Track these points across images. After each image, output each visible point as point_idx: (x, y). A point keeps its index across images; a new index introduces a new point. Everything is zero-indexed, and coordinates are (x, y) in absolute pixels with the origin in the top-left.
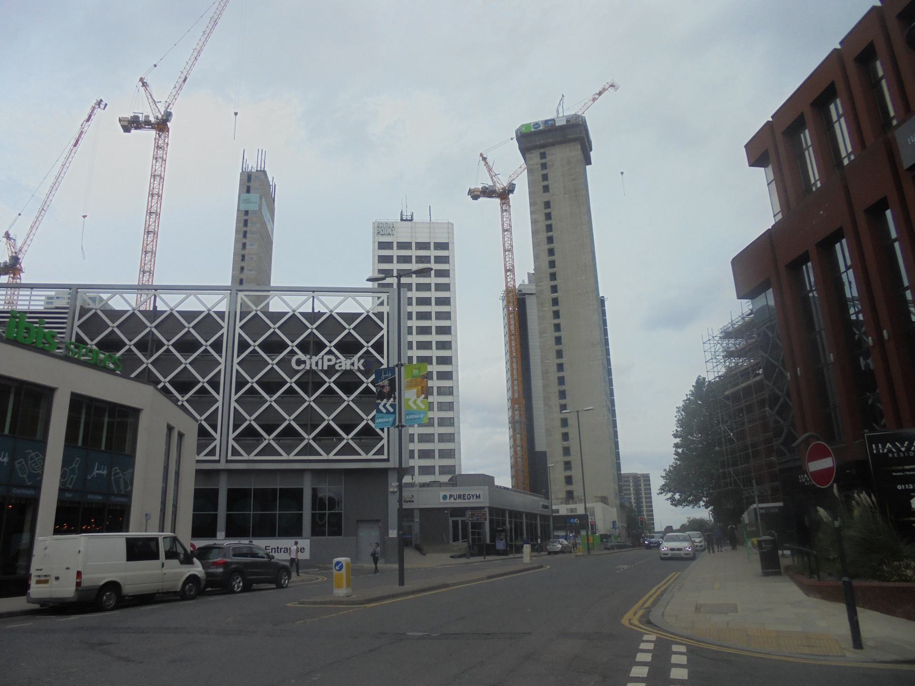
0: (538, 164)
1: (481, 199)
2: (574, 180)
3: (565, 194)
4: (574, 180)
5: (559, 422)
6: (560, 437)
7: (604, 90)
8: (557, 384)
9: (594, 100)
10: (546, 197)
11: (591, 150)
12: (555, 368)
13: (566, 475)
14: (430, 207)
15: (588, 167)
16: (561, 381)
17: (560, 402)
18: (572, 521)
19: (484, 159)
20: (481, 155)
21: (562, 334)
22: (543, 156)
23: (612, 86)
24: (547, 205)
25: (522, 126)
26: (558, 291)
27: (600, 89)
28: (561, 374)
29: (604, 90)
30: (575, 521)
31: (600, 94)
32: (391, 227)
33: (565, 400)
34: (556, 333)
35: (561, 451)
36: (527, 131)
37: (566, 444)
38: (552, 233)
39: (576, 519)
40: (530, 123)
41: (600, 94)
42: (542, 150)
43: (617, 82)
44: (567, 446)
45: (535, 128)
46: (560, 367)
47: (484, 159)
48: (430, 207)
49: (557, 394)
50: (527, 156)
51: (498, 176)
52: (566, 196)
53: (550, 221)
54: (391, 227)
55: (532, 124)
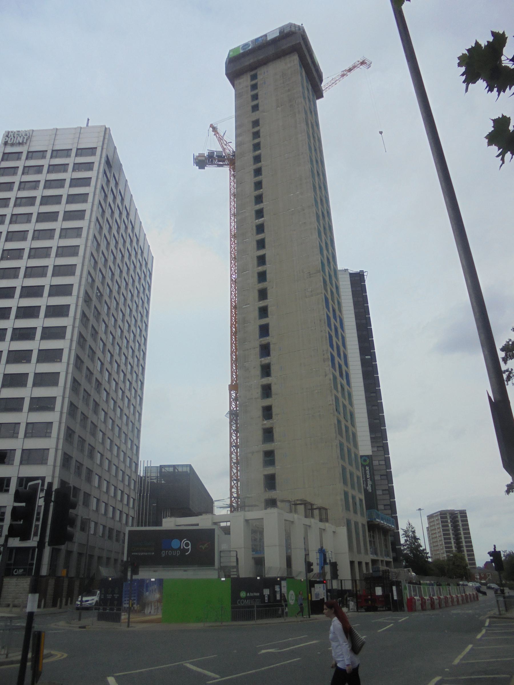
0: (247, 87)
1: (210, 169)
2: (289, 90)
3: (278, 107)
4: (289, 90)
5: (259, 390)
6: (259, 413)
7: (354, 67)
8: (258, 335)
9: (343, 75)
10: (255, 116)
11: (321, 81)
12: (256, 313)
13: (266, 473)
14: (88, 120)
15: (319, 102)
16: (264, 330)
17: (261, 361)
18: (175, 543)
19: (214, 129)
20: (211, 126)
21: (268, 267)
22: (254, 77)
23: (363, 63)
24: (256, 123)
25: (230, 51)
26: (265, 216)
27: (350, 66)
28: (264, 321)
29: (354, 67)
30: (183, 545)
31: (350, 70)
32: (23, 135)
33: (269, 358)
34: (260, 268)
35: (259, 435)
36: (236, 54)
37: (267, 423)
38: (260, 151)
39: (185, 541)
40: (239, 46)
41: (350, 70)
42: (253, 73)
43: (369, 58)
44: (268, 426)
45: (244, 49)
46: (263, 312)
47: (214, 129)
48: (88, 120)
49: (258, 350)
50: (236, 82)
51: (229, 144)
52: (279, 108)
53: (259, 139)
54: (23, 135)
55: (241, 47)
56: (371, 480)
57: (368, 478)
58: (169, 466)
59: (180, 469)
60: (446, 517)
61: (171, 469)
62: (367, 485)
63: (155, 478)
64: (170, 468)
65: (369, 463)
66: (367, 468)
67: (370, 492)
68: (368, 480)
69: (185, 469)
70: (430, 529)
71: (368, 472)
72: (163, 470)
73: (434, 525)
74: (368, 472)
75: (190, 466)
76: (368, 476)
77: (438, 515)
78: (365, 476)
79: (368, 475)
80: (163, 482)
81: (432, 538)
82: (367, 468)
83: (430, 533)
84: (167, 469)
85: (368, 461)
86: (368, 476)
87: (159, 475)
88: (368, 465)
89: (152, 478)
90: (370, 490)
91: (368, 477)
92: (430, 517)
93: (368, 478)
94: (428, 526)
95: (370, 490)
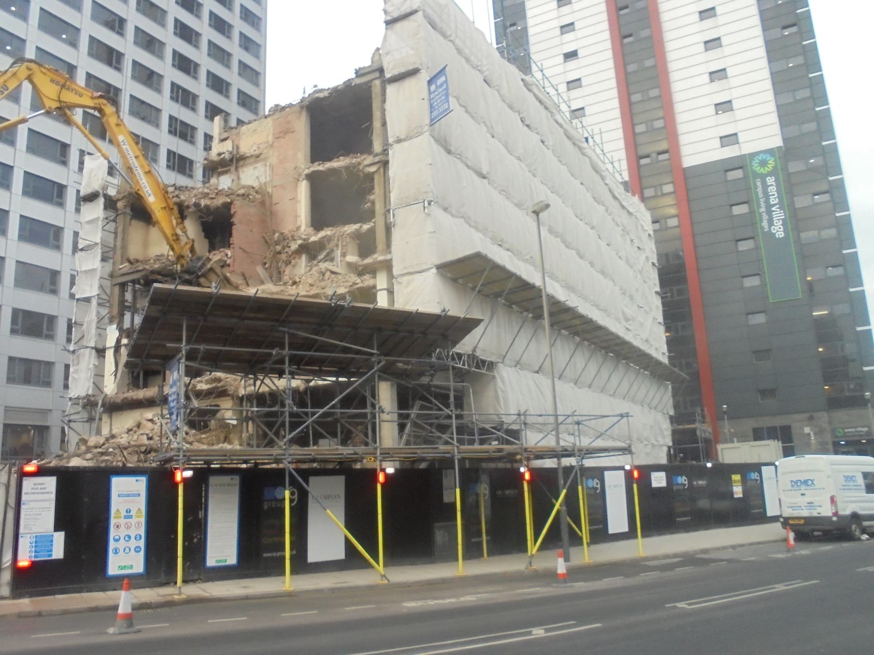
57: (775, 205)
62: (771, 223)
65: (775, 168)
66: (770, 180)
67: (779, 238)
68: (773, 209)
71: (772, 190)
74: (772, 190)
76: (774, 200)
78: (765, 202)
82: (770, 180)
85: (771, 163)
86: (774, 200)
88: (770, 174)
90: (780, 234)
91: (772, 203)
93: (775, 205)
95: (780, 234)
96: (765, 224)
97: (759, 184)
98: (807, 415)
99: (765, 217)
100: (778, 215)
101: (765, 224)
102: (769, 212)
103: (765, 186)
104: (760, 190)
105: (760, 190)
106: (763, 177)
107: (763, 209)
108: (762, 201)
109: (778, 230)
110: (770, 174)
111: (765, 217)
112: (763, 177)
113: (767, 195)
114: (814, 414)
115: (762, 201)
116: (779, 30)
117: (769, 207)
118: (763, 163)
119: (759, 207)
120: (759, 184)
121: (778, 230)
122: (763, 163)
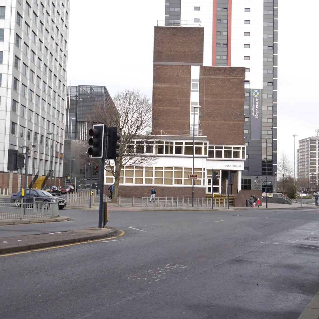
56: (259, 110)
57: (257, 108)
58: (86, 87)
59: (96, 90)
60: (315, 143)
61: (88, 90)
62: (255, 114)
63: (74, 96)
64: (87, 88)
66: (257, 100)
68: (256, 109)
69: (100, 90)
70: (299, 152)
71: (257, 103)
72: (81, 90)
73: (304, 148)
74: (257, 103)
75: (104, 87)
76: (257, 107)
77: (308, 141)
79: (257, 106)
80: (81, 100)
81: (301, 159)
82: (257, 100)
83: (299, 155)
84: (85, 89)
86: (257, 107)
87: (77, 94)
88: (257, 98)
89: (71, 96)
90: (257, 118)
92: (301, 142)
93: (257, 108)
94: (298, 149)
95: (257, 118)
96: (253, 114)
97: (253, 100)
98: (256, 176)
99: (254, 112)
100: (258, 112)
101: (253, 114)
102: (255, 110)
103: (255, 101)
104: (253, 102)
105: (253, 102)
106: (255, 98)
107: (253, 109)
108: (254, 106)
109: (257, 117)
110: (257, 98)
111: (254, 112)
112: (255, 98)
113: (255, 105)
114: (258, 176)
115: (254, 106)
116: (267, 47)
117: (255, 108)
118: (256, 93)
119: (252, 108)
120: (253, 100)
121: (257, 117)
122: (256, 93)
